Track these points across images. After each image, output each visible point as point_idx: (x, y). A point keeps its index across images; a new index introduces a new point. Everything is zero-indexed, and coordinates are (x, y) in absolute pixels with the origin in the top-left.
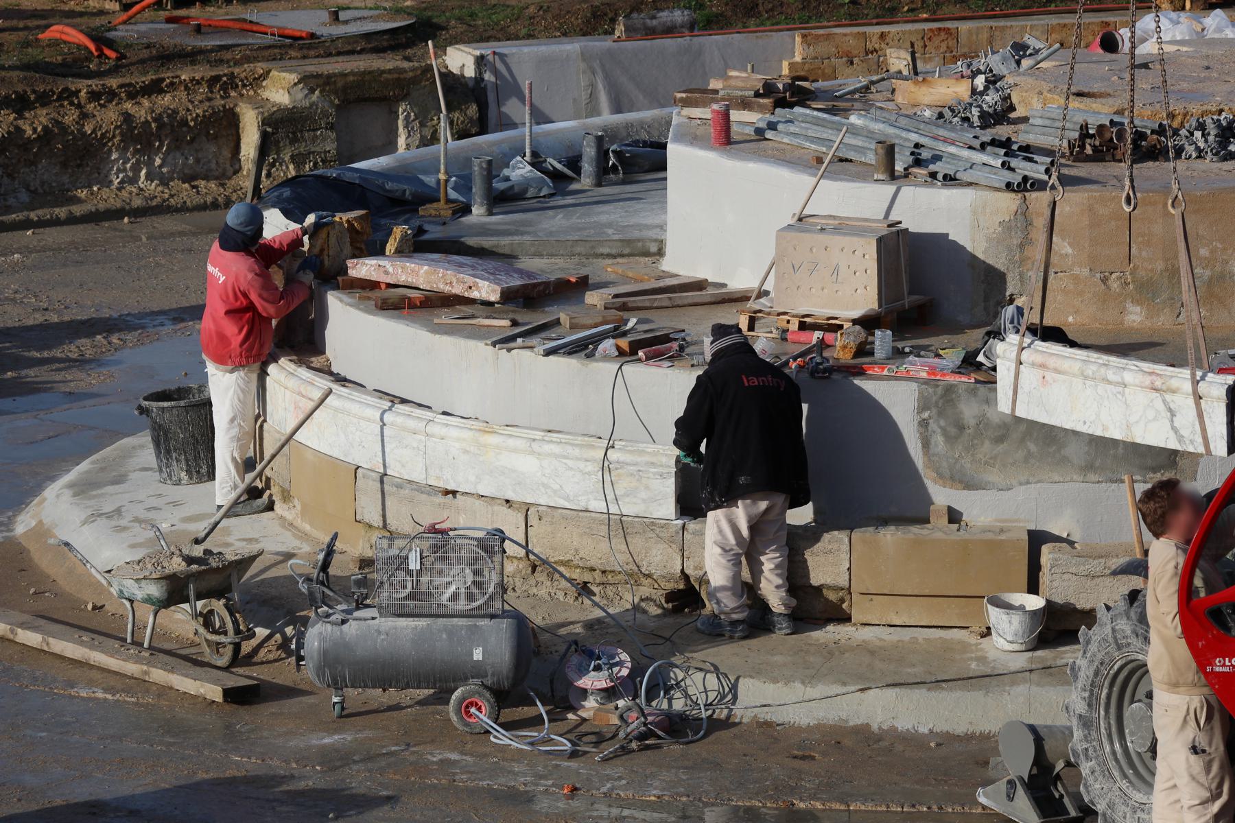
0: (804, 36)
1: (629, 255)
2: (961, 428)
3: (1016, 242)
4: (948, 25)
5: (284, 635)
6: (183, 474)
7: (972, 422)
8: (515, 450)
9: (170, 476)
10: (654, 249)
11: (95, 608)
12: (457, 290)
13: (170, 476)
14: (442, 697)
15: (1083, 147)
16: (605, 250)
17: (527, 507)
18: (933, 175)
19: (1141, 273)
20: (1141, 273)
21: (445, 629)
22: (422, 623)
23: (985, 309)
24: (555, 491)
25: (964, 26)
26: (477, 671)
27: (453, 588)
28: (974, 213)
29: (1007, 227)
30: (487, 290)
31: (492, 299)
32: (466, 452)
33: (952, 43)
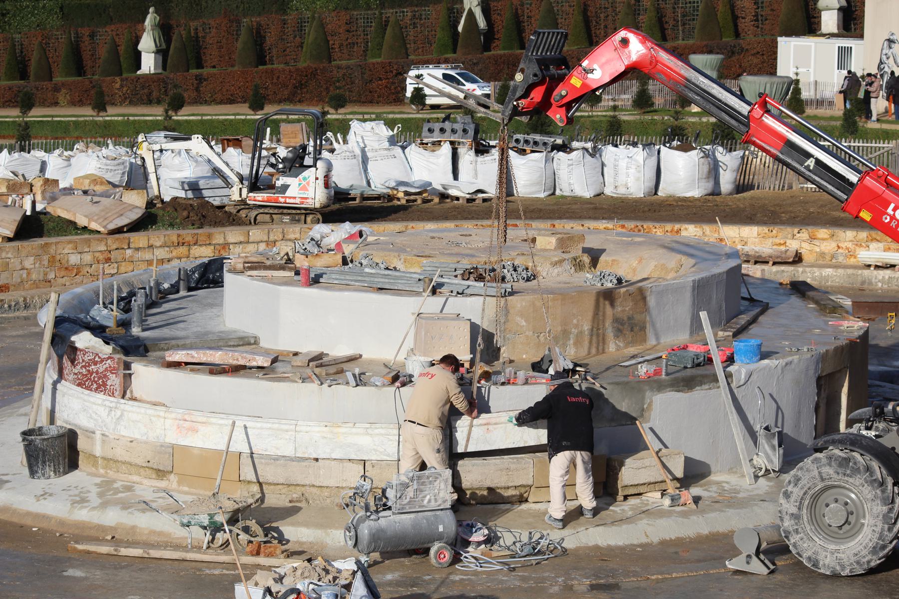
1: (243, 345)
6: (52, 473)
8: (357, 434)
10: (252, 341)
11: (113, 537)
13: (43, 475)
14: (426, 551)
16: (232, 343)
21: (424, 518)
22: (412, 516)
23: (488, 354)
24: (381, 452)
26: (440, 538)
31: (265, 365)
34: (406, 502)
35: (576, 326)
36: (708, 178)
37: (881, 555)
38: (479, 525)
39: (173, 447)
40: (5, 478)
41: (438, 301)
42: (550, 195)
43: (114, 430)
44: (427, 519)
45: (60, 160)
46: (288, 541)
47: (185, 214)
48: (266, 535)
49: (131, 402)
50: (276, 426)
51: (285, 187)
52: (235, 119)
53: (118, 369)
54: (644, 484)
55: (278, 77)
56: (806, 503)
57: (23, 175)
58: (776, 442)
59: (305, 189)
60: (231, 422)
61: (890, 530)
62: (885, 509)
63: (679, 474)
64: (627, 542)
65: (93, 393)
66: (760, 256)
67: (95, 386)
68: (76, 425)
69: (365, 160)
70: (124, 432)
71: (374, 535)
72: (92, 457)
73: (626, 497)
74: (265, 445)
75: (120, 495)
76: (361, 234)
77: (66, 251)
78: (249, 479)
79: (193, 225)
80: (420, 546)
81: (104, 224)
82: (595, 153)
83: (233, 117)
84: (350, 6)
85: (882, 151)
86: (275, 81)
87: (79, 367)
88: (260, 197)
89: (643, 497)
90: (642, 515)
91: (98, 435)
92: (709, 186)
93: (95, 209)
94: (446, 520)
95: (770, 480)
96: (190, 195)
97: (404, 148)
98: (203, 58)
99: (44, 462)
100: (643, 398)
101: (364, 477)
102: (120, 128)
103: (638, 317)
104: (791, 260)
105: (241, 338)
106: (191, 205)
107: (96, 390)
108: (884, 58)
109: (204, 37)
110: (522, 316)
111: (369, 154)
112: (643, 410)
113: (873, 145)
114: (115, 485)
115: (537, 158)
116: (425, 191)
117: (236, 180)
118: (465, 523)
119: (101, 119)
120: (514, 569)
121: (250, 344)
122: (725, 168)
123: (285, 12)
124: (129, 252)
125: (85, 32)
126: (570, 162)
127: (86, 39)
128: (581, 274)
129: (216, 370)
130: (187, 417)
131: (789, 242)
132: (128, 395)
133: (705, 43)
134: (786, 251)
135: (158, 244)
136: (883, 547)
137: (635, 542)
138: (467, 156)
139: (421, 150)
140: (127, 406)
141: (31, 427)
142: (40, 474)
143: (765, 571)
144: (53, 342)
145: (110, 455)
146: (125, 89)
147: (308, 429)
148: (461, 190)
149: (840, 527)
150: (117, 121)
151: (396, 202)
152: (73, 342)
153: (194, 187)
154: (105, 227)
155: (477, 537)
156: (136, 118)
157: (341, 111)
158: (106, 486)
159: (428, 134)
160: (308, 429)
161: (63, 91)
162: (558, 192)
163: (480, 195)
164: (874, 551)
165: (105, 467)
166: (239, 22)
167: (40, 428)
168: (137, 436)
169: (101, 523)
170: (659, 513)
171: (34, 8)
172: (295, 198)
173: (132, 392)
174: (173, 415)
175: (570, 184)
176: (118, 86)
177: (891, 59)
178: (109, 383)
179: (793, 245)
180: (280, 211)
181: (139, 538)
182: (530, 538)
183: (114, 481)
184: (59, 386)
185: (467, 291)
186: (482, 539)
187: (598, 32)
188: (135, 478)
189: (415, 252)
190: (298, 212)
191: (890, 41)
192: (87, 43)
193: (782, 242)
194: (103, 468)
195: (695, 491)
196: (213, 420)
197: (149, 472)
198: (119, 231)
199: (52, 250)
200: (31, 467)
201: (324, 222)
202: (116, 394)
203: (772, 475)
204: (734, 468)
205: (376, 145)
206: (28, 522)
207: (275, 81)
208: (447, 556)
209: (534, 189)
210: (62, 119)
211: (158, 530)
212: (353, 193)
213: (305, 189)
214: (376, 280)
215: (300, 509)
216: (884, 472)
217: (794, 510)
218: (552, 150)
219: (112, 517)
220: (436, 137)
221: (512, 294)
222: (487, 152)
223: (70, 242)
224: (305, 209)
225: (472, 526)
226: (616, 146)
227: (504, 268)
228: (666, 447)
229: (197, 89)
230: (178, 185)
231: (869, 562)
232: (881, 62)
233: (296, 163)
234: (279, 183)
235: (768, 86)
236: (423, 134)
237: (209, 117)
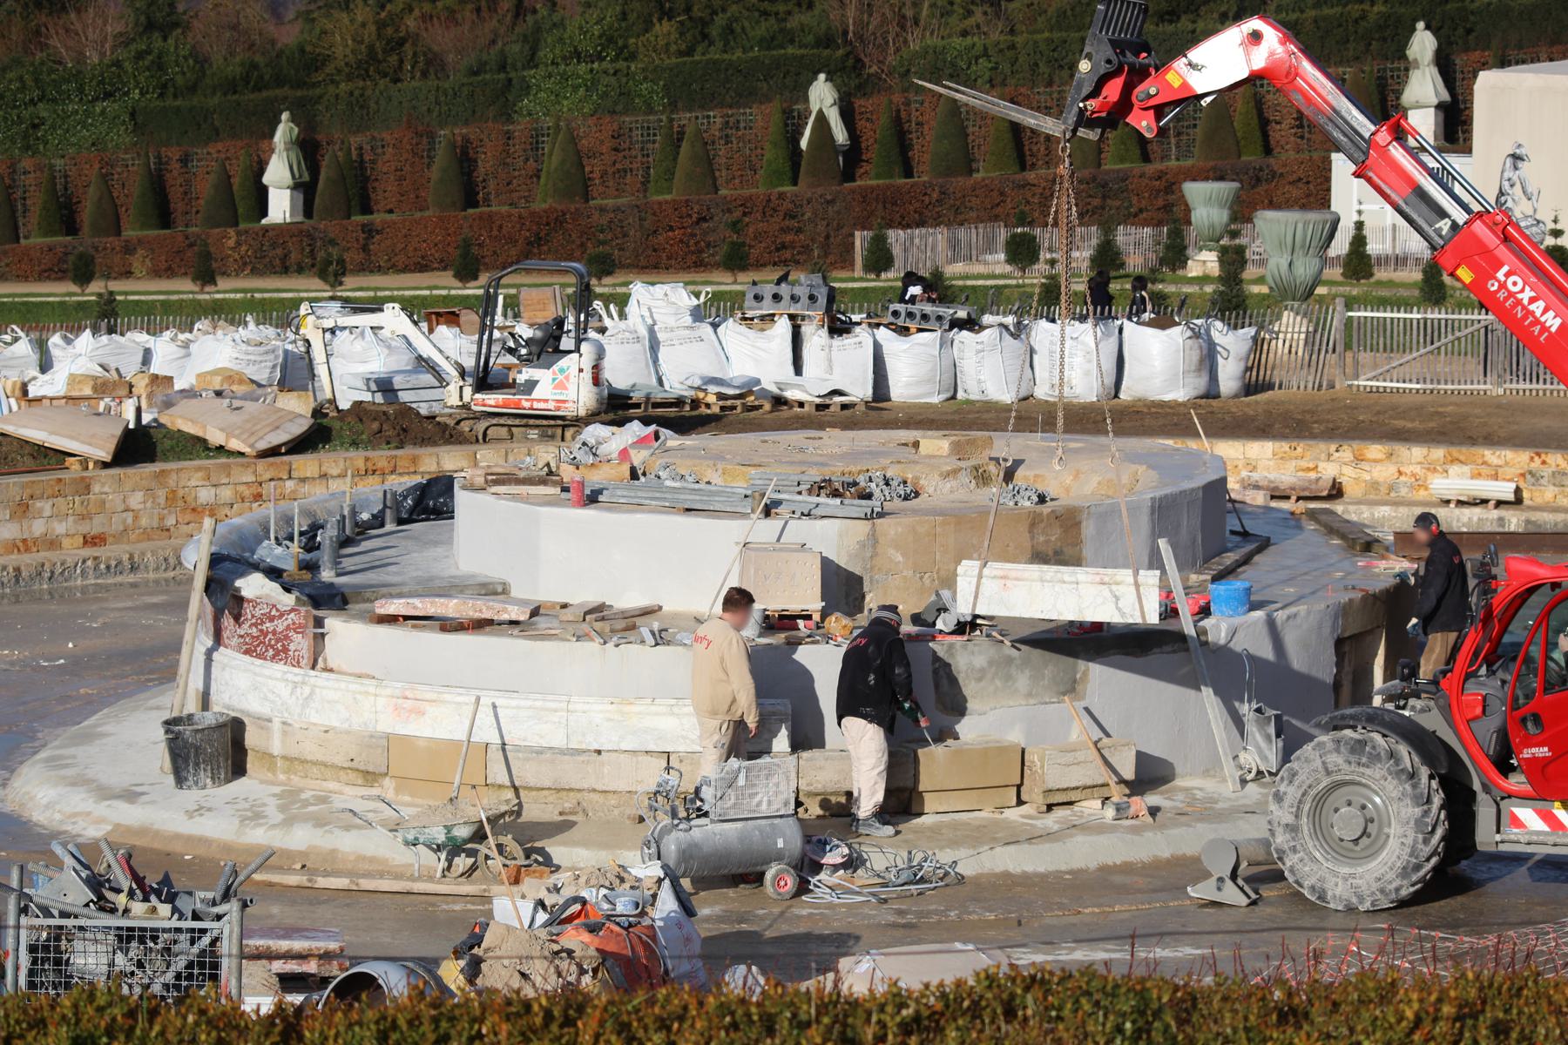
6: (209, 781)
8: (657, 714)
12: (487, 615)
13: (196, 783)
14: (758, 878)
19: (942, 573)
20: (942, 573)
22: (739, 825)
26: (779, 857)
28: (840, 535)
29: (863, 545)
32: (609, 720)
34: (730, 803)
36: (1199, 370)
37: (1414, 878)
38: (836, 842)
39: (388, 737)
40: (139, 789)
41: (773, 525)
43: (300, 715)
45: (173, 347)
47: (375, 426)
48: (528, 857)
49: (325, 675)
50: (539, 704)
51: (531, 385)
53: (305, 627)
55: (501, 227)
56: (1306, 808)
58: (1272, 730)
61: (1426, 841)
62: (1418, 811)
63: (1129, 773)
64: (1051, 868)
65: (269, 663)
66: (1276, 488)
67: (271, 652)
68: (242, 711)
69: (654, 346)
70: (315, 718)
72: (268, 757)
73: (1050, 807)
75: (311, 808)
77: (193, 483)
78: (499, 781)
80: (750, 869)
81: (252, 440)
82: (1018, 332)
83: (427, 292)
84: (619, 108)
85: (1476, 326)
86: (495, 233)
87: (246, 626)
88: (492, 400)
89: (1076, 808)
90: (1074, 831)
91: (276, 725)
92: (1199, 384)
93: (235, 418)
94: (788, 832)
95: (1264, 785)
96: (379, 398)
97: (715, 326)
98: (373, 196)
99: (197, 764)
101: (668, 769)
104: (1325, 493)
105: (483, 585)
106: (385, 413)
107: (273, 658)
108: (1506, 185)
109: (373, 162)
110: (897, 548)
111: (660, 336)
112: (1075, 681)
113: (1463, 317)
114: (303, 796)
116: (750, 392)
117: (455, 373)
118: (814, 839)
119: (207, 297)
120: (885, 901)
121: (496, 593)
122: (1225, 354)
123: (509, 120)
124: (290, 484)
125: (174, 153)
126: (979, 347)
127: (175, 166)
129: (449, 626)
130: (409, 694)
131: (1321, 465)
132: (320, 664)
133: (1212, 163)
134: (1318, 480)
135: (335, 472)
136: (1417, 867)
137: (1064, 868)
138: (816, 338)
139: (743, 329)
140: (317, 678)
141: (175, 714)
142: (190, 782)
143: (1244, 901)
144: (208, 589)
145: (294, 751)
146: (244, 248)
147: (586, 707)
148: (805, 390)
149: (1356, 841)
151: (703, 410)
152: (238, 590)
153: (385, 386)
154: (252, 446)
155: (833, 857)
156: (266, 295)
158: (289, 798)
159: (754, 303)
160: (586, 707)
161: (140, 252)
162: (960, 395)
163: (838, 399)
164: (1405, 873)
165: (287, 772)
166: (432, 136)
167: (190, 716)
168: (335, 723)
170: (1098, 828)
171: (87, 114)
172: (546, 401)
173: (325, 660)
174: (388, 691)
175: (979, 381)
176: (231, 243)
177: (1518, 186)
178: (292, 647)
179: (1328, 471)
180: (524, 421)
182: (910, 860)
183: (301, 790)
184: (215, 656)
186: (840, 860)
187: (1035, 148)
188: (332, 785)
189: (739, 459)
191: (1516, 158)
192: (175, 173)
193: (1311, 465)
195: (1153, 799)
196: (447, 697)
197: (352, 776)
198: (273, 452)
199: (172, 481)
202: (303, 662)
203: (1268, 779)
204: (1212, 768)
205: (671, 322)
206: (177, 847)
207: (495, 233)
208: (790, 882)
210: (143, 298)
211: (369, 854)
212: (637, 396)
213: (562, 386)
215: (573, 824)
216: (1416, 759)
217: (1289, 819)
218: (951, 328)
219: (300, 838)
220: (767, 308)
221: (881, 515)
222: (848, 331)
223: (199, 469)
224: (562, 418)
225: (826, 843)
226: (1053, 321)
228: (1108, 735)
229: (365, 248)
230: (361, 384)
231: (1397, 890)
232: (1501, 193)
233: (547, 347)
234: (521, 378)
235: (1300, 226)
236: (746, 304)
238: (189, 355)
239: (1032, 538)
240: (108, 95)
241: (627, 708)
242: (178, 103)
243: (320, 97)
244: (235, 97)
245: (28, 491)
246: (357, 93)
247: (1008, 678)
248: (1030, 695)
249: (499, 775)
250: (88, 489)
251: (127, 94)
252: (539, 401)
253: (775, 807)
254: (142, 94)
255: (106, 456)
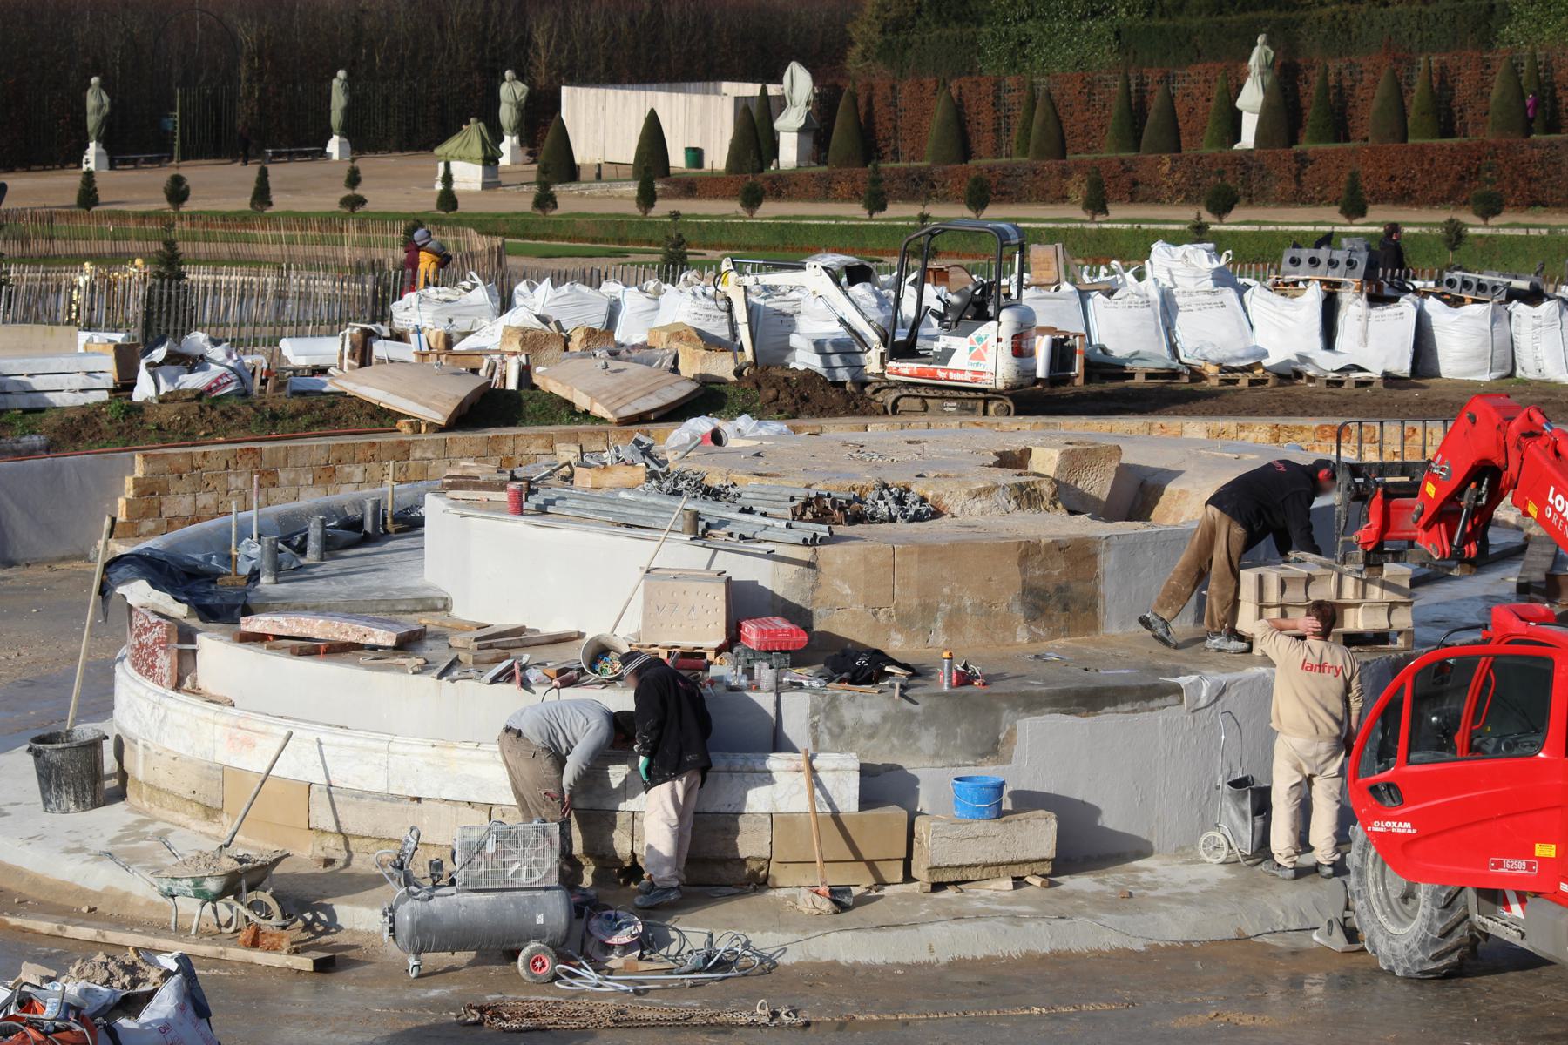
0: (145, 456)
2: (843, 728)
3: (808, 585)
4: (256, 445)
5: (304, 919)
6: (72, 804)
7: (851, 723)
9: (59, 806)
10: (440, 605)
11: (90, 910)
13: (59, 806)
14: (513, 955)
15: (803, 514)
16: (403, 607)
17: (490, 807)
18: (731, 535)
19: (901, 608)
21: (511, 900)
22: (492, 896)
25: (266, 446)
26: (538, 934)
27: (517, 866)
30: (384, 637)
32: (430, 764)
33: (257, 460)
35: (949, 599)
39: (223, 768)
42: (1503, 377)
44: (517, 904)
45: (642, 298)
46: (340, 928)
47: (771, 393)
50: (360, 742)
51: (948, 354)
52: (1259, 232)
53: (167, 641)
54: (976, 866)
57: (558, 323)
59: (982, 356)
60: (285, 732)
71: (418, 924)
73: (938, 887)
74: (348, 774)
76: (716, 437)
77: (533, 450)
79: (780, 412)
81: (616, 406)
83: (1310, 228)
88: (905, 369)
93: (608, 381)
94: (551, 907)
99: (59, 786)
100: (997, 722)
102: (1123, 243)
103: (1078, 588)
105: (420, 600)
106: (786, 380)
109: (1352, 87)
110: (844, 579)
111: (1179, 300)
112: (997, 741)
115: (1476, 313)
116: (1259, 365)
119: (1094, 226)
121: (435, 609)
123: (1490, 48)
125: (1153, 76)
126: (1537, 322)
128: (1028, 513)
129: (309, 648)
130: (241, 723)
132: (188, 685)
139: (1274, 297)
142: (53, 806)
146: (1178, 175)
147: (407, 749)
150: (1118, 230)
155: (622, 938)
156: (1153, 226)
157: (1492, 221)
159: (1291, 268)
160: (407, 749)
161: (1077, 177)
162: (1519, 373)
163: (1355, 375)
166: (1412, 63)
168: (182, 751)
169: (84, 886)
171: (1073, 32)
172: (962, 371)
173: (195, 680)
176: (1166, 169)
180: (939, 393)
181: (128, 912)
185: (758, 536)
186: (627, 940)
188: (181, 818)
190: (972, 394)
194: (148, 800)
197: (196, 808)
198: (641, 419)
199: (507, 449)
200: (44, 791)
201: (1017, 414)
202: (165, 680)
205: (1190, 285)
207: (1426, 167)
209: (1472, 366)
210: (1033, 225)
212: (1136, 366)
214: (629, 511)
218: (1509, 299)
221: (823, 541)
223: (540, 436)
224: (985, 391)
225: (616, 920)
227: (881, 497)
229: (1299, 182)
233: (976, 310)
236: (1283, 268)
237: (1271, 228)
238: (657, 308)
239: (1024, 571)
240: (1095, 14)
241: (447, 753)
242: (1162, 23)
243: (1303, 20)
244: (1220, 18)
245: (334, 455)
246: (1339, 17)
247: (909, 735)
248: (936, 756)
249: (324, 820)
250: (407, 454)
251: (1114, 12)
252: (955, 371)
253: (538, 877)
254: (1129, 13)
255: (441, 419)
